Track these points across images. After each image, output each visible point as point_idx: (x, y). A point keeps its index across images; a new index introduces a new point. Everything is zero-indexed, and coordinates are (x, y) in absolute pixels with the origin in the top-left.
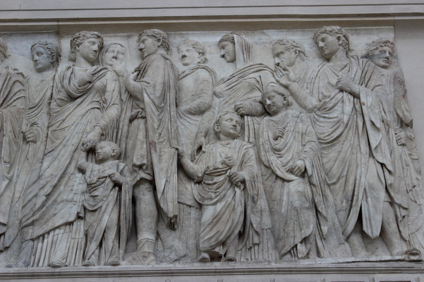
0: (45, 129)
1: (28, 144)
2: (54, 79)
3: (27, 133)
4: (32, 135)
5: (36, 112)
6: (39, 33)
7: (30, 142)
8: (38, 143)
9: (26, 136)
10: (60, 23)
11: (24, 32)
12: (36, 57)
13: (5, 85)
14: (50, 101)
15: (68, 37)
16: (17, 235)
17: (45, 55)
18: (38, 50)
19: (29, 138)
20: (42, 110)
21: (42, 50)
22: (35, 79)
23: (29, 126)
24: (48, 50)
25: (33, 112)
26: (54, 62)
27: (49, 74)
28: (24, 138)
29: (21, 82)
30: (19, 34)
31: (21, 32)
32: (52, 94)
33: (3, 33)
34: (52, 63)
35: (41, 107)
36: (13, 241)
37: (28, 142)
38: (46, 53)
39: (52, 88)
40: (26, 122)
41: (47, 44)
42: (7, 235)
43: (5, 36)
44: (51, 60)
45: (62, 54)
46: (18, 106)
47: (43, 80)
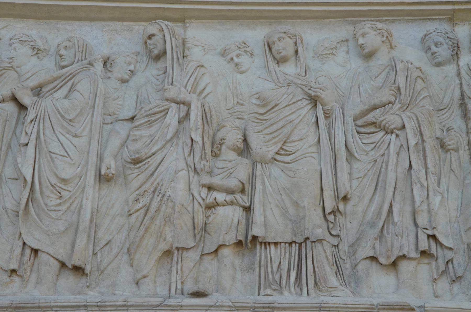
0: (464, 135)
1: (449, 153)
2: (459, 74)
3: (447, 139)
4: (453, 141)
5: (447, 114)
6: (429, 19)
7: (451, 151)
8: (461, 152)
9: (444, 143)
10: (457, 7)
11: (409, 18)
12: (434, 49)
13: (408, 82)
14: (461, 102)
15: (464, 25)
16: (468, 262)
17: (445, 46)
18: (436, 40)
19: (449, 145)
20: (453, 112)
21: (441, 40)
22: (435, 75)
23: (445, 132)
24: (449, 39)
25: (443, 114)
26: (454, 55)
27: (451, 69)
28: (443, 145)
29: (422, 79)
30: (403, 20)
31: (406, 18)
32: (462, 93)
33: (384, 18)
34: (452, 55)
35: (451, 110)
36: (465, 269)
37: (449, 150)
38: (446, 43)
39: (459, 86)
40: (439, 126)
41: (447, 33)
42: (455, 262)
43: (387, 22)
44: (451, 53)
45: (460, 46)
46: (427, 107)
47: (446, 76)
